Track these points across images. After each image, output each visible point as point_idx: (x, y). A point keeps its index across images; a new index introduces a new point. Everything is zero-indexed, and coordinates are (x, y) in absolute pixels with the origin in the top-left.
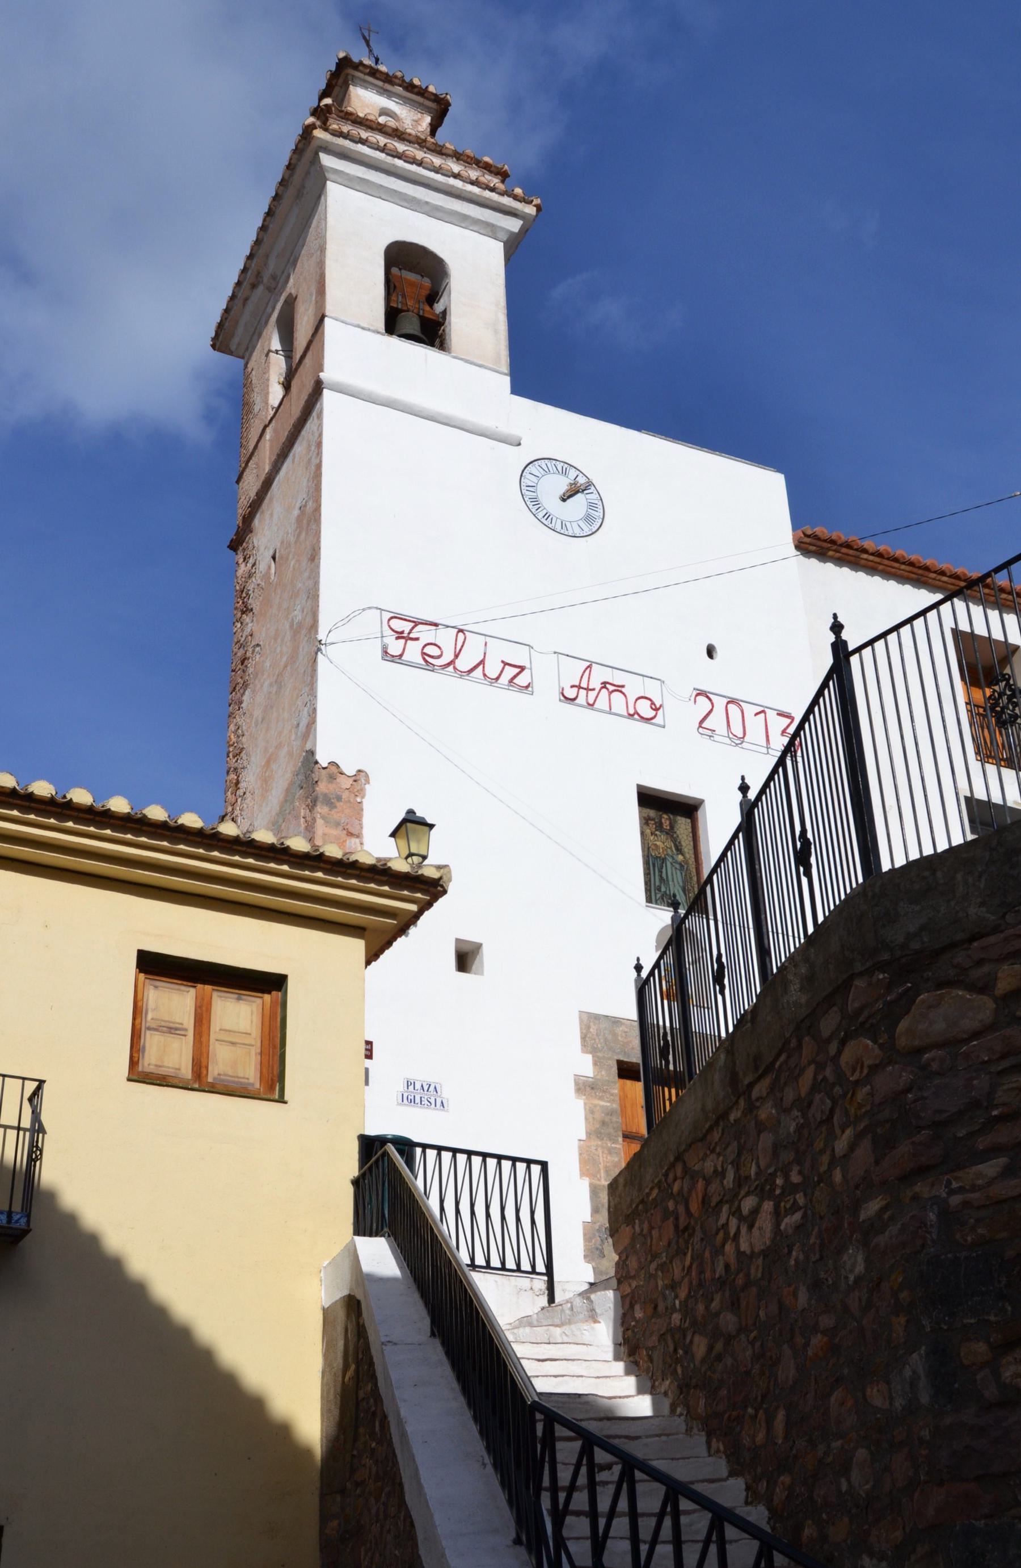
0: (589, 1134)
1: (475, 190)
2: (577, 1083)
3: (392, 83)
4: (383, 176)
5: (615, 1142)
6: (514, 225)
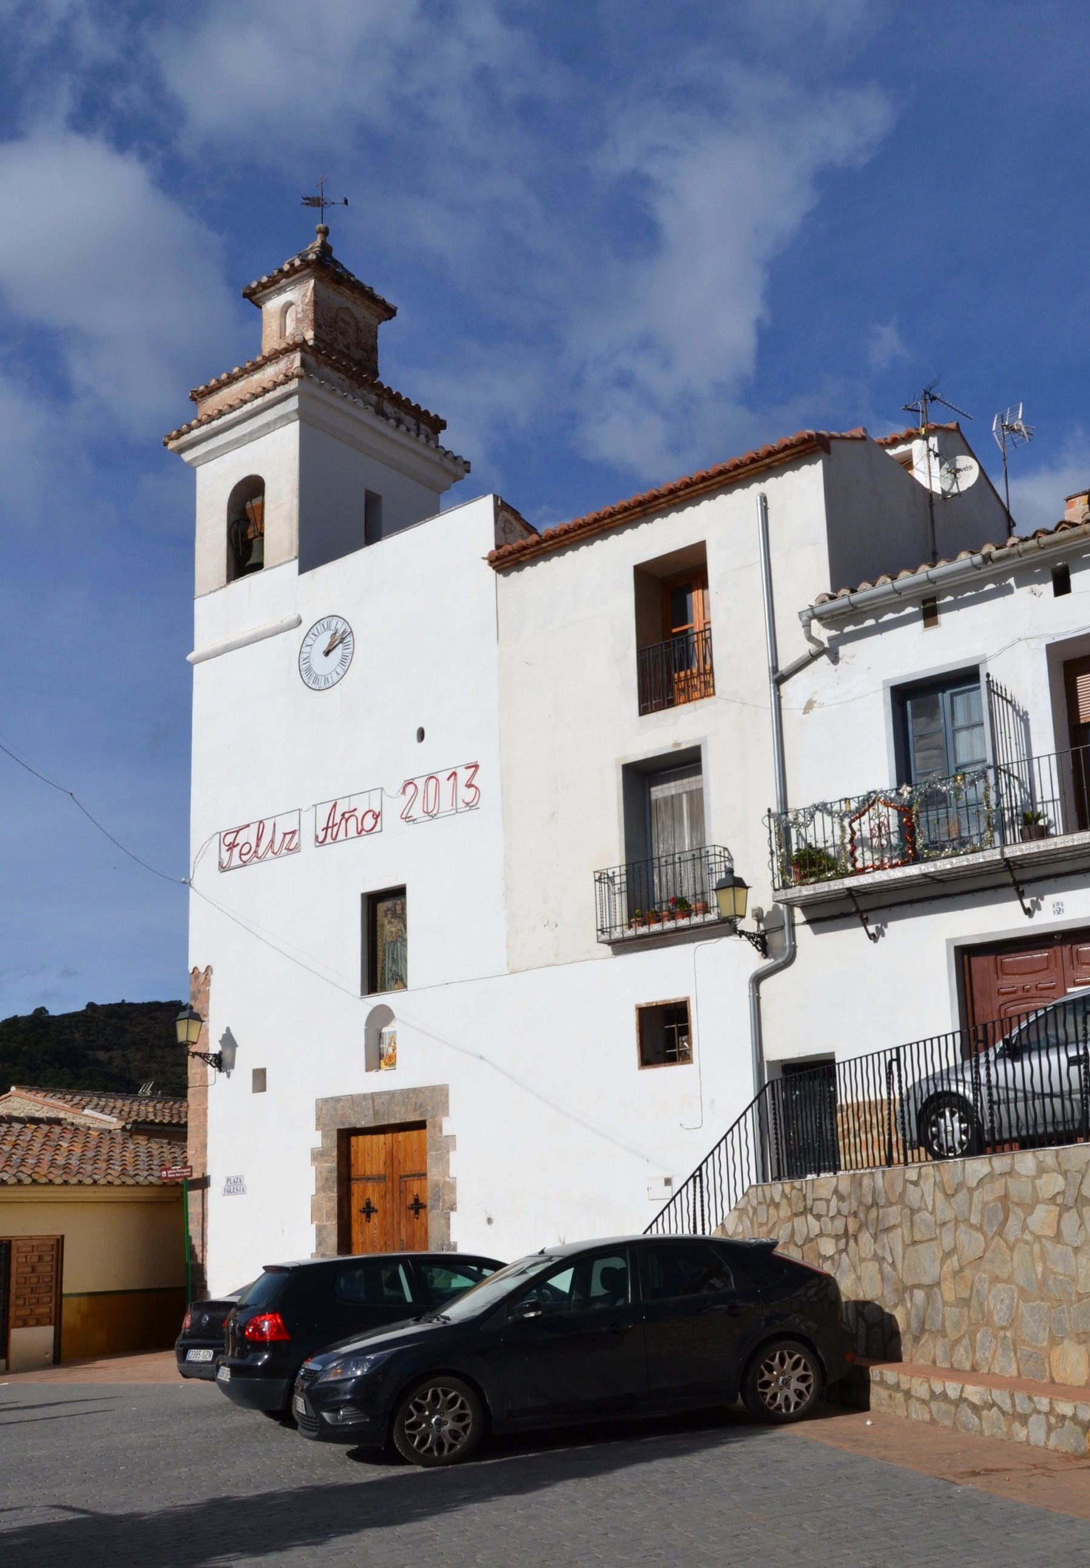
0: (317, 1190)
1: (259, 401)
2: (312, 1153)
3: (277, 282)
4: (215, 439)
5: (333, 1192)
6: (293, 403)
